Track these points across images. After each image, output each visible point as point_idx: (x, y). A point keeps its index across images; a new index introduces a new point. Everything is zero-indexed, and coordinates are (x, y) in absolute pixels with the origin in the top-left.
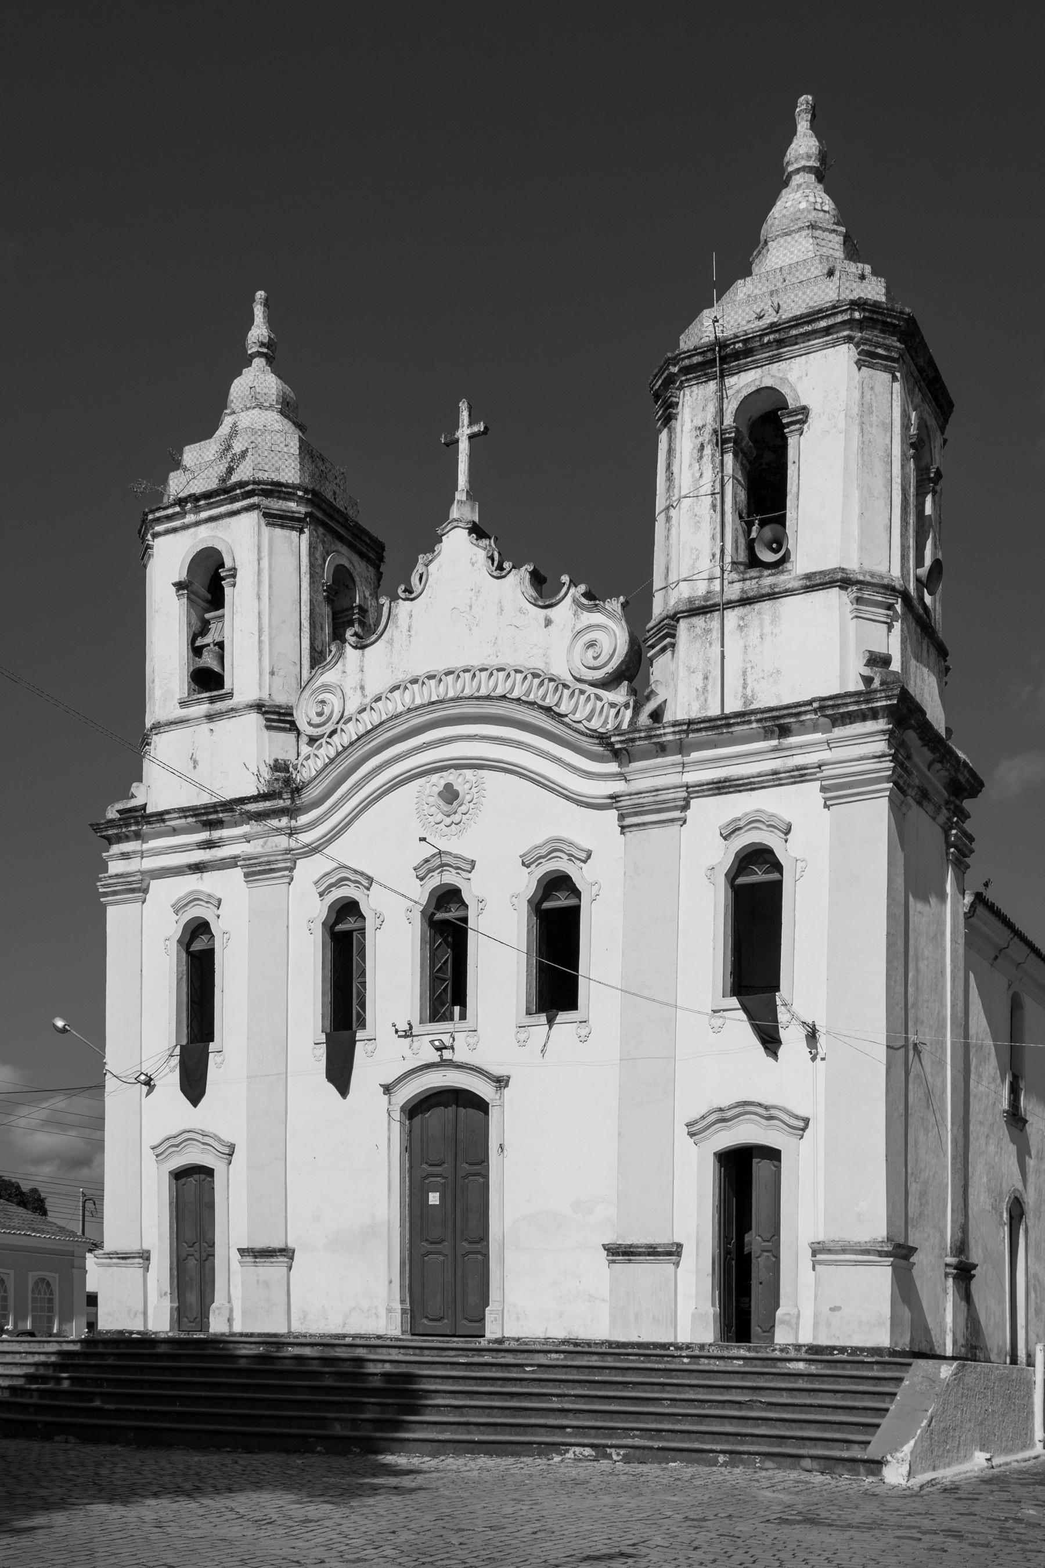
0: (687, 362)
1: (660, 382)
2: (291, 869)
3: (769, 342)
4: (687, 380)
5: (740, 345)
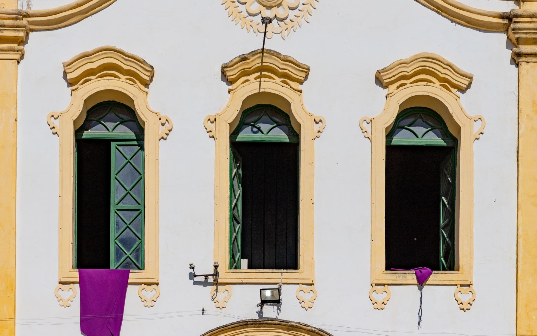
2: (23, 42)
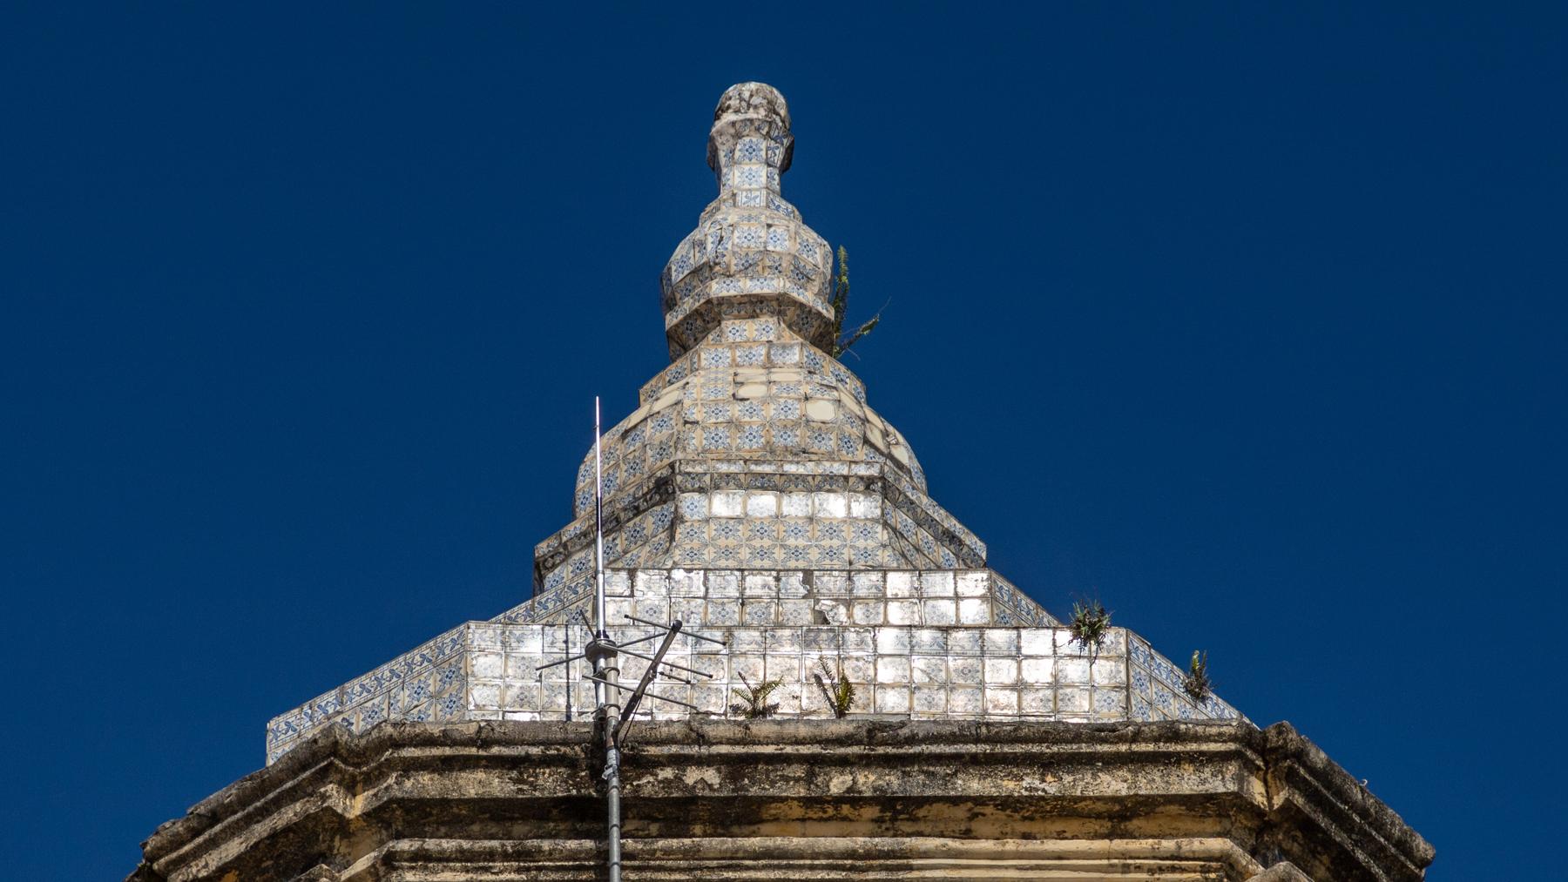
0: (427, 784)
1: (234, 848)
3: (852, 798)
5: (711, 776)
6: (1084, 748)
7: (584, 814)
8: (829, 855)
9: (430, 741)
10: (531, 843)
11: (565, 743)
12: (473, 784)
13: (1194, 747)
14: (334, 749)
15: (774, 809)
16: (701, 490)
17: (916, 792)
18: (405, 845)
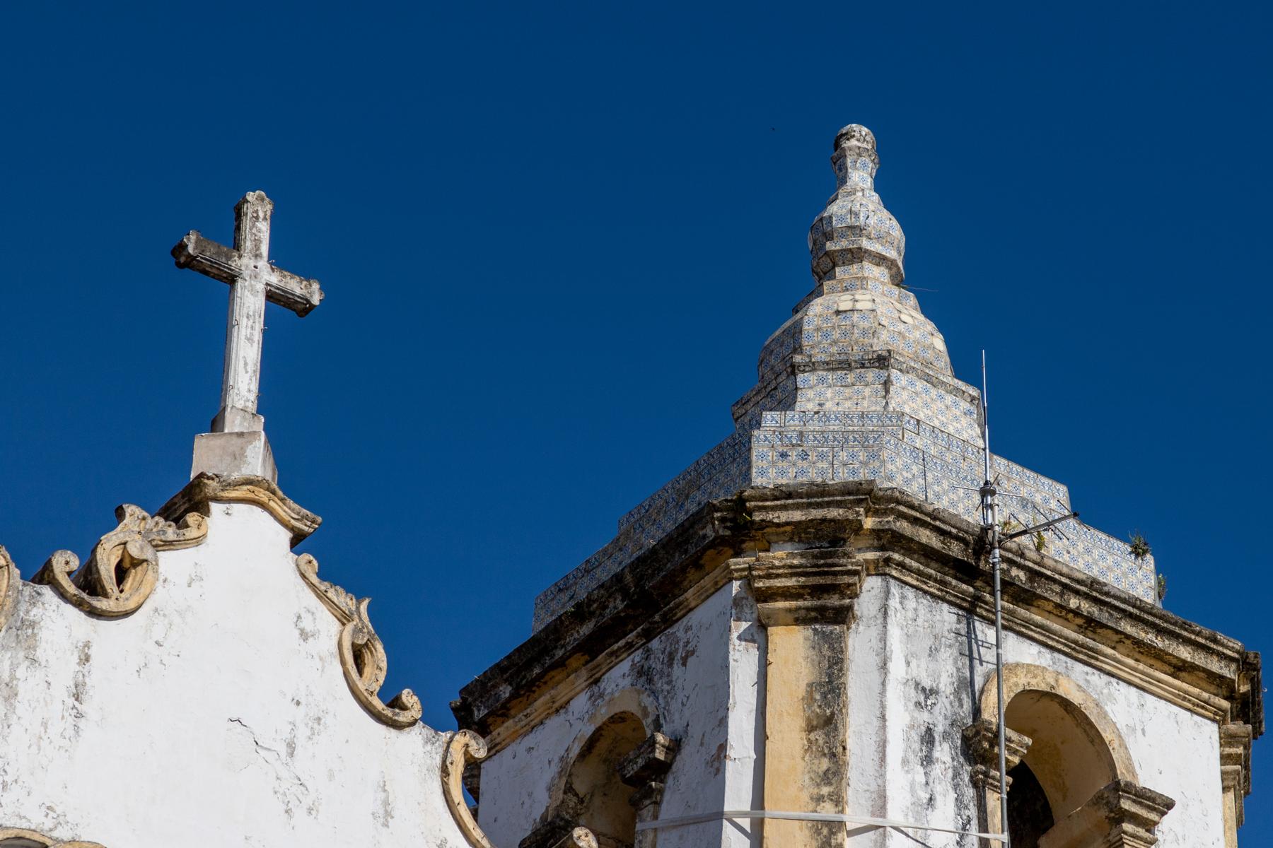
0: (904, 527)
1: (797, 516)
3: (1076, 613)
4: (902, 566)
5: (1022, 575)
6: (1177, 630)
7: (967, 572)
8: (1067, 639)
9: (912, 507)
10: (948, 579)
11: (966, 532)
12: (926, 537)
13: (1220, 649)
14: (870, 492)
15: (1041, 603)
16: (901, 370)
17: (1105, 621)
18: (896, 556)
